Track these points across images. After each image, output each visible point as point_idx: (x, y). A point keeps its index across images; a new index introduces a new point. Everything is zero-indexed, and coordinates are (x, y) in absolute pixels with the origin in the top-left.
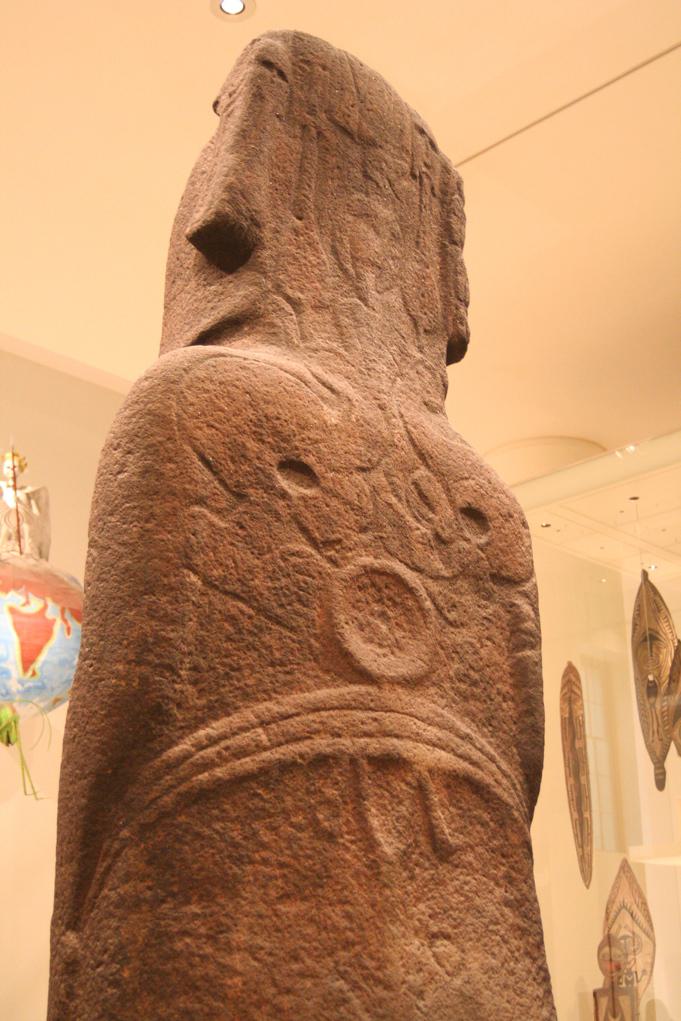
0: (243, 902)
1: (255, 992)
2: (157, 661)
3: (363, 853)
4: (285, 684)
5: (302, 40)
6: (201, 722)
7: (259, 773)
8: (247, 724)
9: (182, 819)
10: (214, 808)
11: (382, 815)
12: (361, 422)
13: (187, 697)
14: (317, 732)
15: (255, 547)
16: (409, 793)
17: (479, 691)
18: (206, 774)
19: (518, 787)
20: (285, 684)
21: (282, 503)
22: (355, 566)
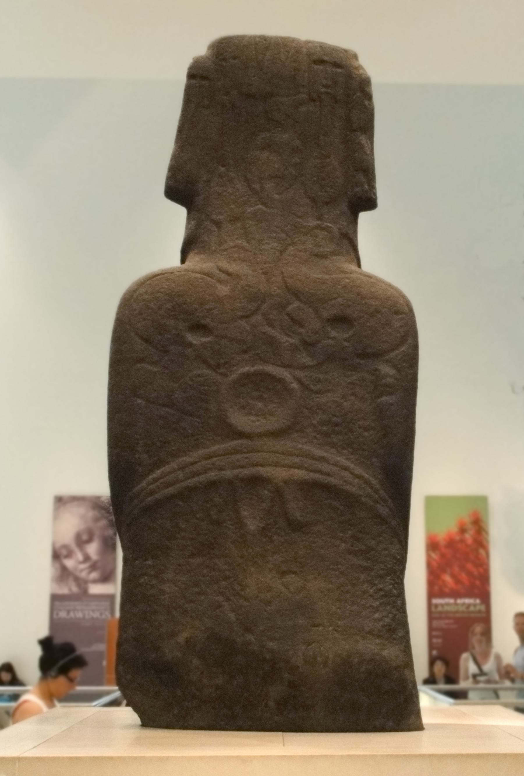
0: (171, 558)
5: (222, 43)
6: (151, 471)
12: (247, 288)
14: (210, 469)
19: (374, 481)
21: (190, 350)
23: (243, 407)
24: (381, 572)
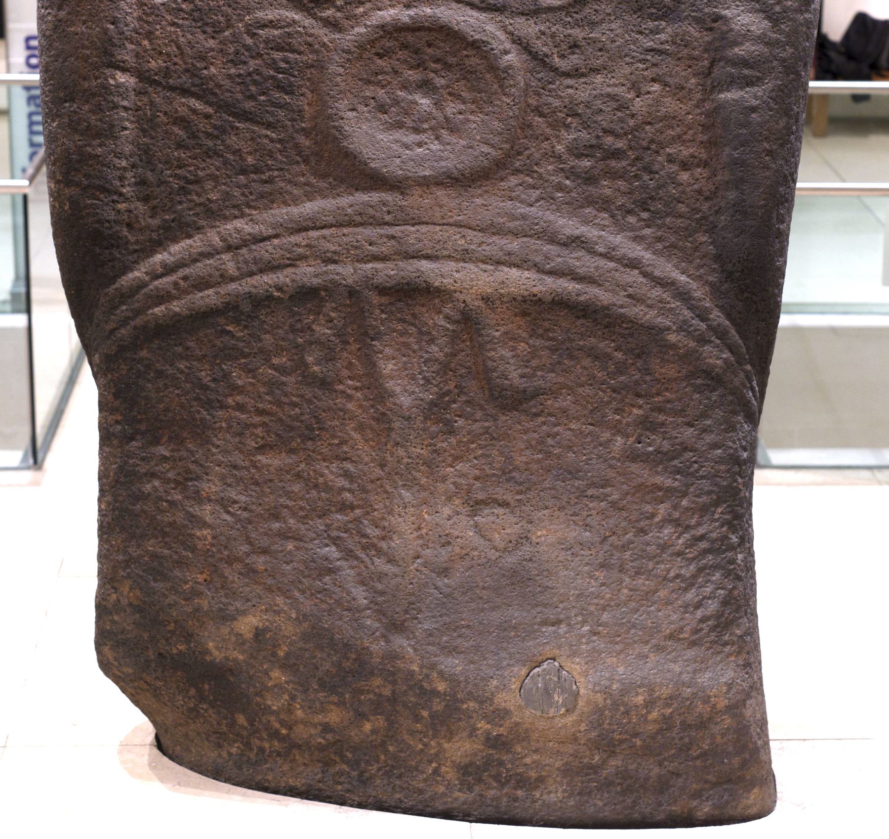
1: (226, 547)
2: (86, 183)
3: (371, 403)
4: (261, 196)
6: (157, 245)
7: (225, 308)
8: (209, 249)
9: (144, 353)
10: (176, 345)
11: (404, 356)
13: (137, 217)
14: (302, 257)
15: (207, 24)
16: (448, 329)
17: (624, 163)
18: (163, 307)
19: (698, 291)
20: (261, 196)
22: (366, 26)
23: (382, 108)
24: (704, 499)
